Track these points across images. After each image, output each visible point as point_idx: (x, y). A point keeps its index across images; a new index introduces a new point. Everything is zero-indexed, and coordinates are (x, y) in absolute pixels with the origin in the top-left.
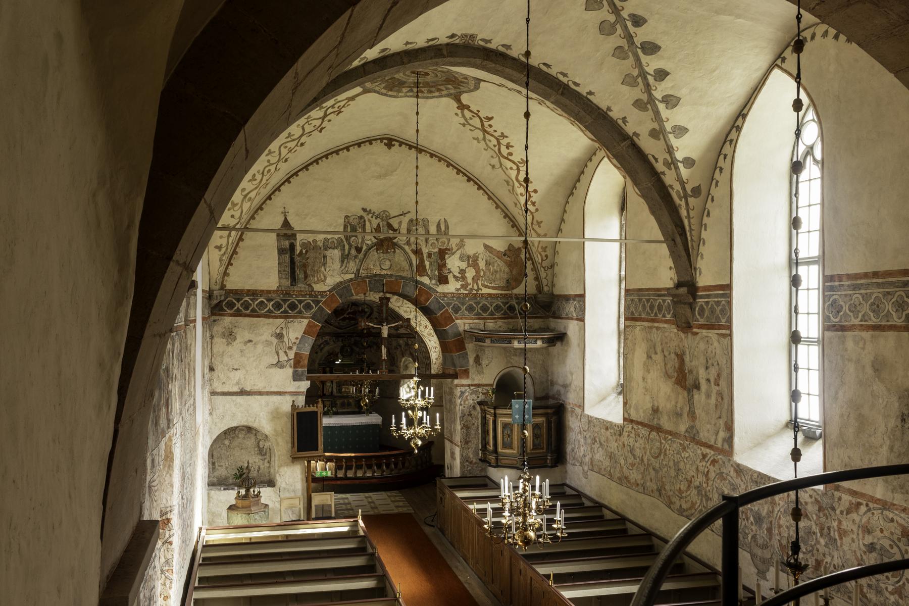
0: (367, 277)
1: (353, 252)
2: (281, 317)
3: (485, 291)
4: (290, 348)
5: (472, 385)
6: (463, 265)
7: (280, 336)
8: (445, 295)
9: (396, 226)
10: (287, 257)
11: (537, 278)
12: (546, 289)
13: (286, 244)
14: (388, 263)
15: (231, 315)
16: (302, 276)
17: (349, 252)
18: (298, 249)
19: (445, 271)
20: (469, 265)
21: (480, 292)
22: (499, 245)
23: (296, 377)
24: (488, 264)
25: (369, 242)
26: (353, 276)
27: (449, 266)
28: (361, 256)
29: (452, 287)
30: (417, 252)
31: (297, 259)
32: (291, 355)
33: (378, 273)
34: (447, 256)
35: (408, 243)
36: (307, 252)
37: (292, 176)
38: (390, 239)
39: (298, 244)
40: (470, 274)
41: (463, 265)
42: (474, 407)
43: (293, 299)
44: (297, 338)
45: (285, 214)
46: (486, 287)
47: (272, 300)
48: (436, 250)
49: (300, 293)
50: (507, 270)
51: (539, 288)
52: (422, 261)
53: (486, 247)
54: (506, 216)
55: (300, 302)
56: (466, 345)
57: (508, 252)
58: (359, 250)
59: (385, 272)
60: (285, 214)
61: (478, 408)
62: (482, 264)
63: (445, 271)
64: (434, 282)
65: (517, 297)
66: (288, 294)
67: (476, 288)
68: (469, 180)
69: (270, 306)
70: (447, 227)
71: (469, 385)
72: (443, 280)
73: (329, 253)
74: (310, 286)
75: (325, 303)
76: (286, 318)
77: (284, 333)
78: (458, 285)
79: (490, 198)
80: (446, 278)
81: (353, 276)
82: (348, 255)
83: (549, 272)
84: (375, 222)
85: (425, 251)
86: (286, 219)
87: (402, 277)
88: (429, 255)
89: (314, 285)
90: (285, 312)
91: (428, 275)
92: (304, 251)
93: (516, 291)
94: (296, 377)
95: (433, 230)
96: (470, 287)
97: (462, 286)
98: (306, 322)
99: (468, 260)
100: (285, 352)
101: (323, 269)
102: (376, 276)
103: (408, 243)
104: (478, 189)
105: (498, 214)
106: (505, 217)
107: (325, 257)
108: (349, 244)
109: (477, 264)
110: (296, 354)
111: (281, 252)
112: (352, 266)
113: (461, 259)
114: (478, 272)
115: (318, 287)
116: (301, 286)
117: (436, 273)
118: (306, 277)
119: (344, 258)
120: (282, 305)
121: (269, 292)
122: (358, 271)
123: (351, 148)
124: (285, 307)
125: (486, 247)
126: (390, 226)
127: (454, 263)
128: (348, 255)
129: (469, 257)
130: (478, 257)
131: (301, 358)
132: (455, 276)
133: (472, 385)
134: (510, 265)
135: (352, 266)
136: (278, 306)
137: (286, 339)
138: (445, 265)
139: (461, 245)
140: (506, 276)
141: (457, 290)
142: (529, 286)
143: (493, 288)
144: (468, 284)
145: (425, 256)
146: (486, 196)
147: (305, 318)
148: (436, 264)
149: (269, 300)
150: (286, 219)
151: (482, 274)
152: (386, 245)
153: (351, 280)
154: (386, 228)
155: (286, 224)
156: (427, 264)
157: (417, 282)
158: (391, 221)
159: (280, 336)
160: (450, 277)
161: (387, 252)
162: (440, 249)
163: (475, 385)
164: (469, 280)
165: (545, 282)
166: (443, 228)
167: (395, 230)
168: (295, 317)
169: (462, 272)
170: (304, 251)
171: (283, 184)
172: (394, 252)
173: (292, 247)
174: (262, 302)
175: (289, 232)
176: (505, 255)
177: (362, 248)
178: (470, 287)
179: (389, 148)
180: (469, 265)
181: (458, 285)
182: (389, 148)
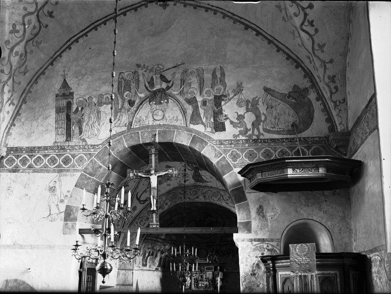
0: (139, 129)
1: (127, 105)
2: (54, 171)
3: (268, 136)
4: (62, 201)
5: (255, 240)
6: (242, 111)
7: (52, 189)
8: (221, 142)
9: (169, 77)
10: (63, 116)
11: (330, 120)
12: (340, 128)
13: (64, 103)
14: (160, 113)
15: (10, 171)
16: (77, 131)
17: (122, 107)
18: (74, 107)
19: (221, 118)
20: (248, 110)
21: (261, 137)
22: (283, 88)
23: (66, 230)
24: (270, 107)
25: (142, 95)
26: (125, 128)
27: (225, 113)
28: (134, 109)
29: (230, 132)
30: (192, 101)
31: (73, 116)
32: (63, 208)
33: (151, 124)
34: (223, 103)
35: (181, 93)
36: (82, 109)
37: (72, 43)
38: (162, 91)
39: (75, 102)
40: (249, 118)
41: (242, 111)
42: (258, 265)
43: (68, 154)
44: (68, 192)
45: (64, 76)
46: (268, 131)
47: (49, 155)
48: (212, 97)
49: (73, 148)
50: (292, 112)
51: (332, 128)
52: (196, 109)
53: (267, 90)
54: (289, 57)
55: (74, 156)
56: (247, 195)
57: (291, 94)
58: (131, 103)
59: (158, 123)
60: (64, 76)
61: (262, 266)
62: (262, 109)
63: (221, 118)
64: (209, 129)
65: (305, 140)
66: (63, 148)
67: (256, 132)
68: (247, 27)
69: (46, 161)
70: (223, 74)
71: (251, 240)
72: (219, 127)
73: (102, 109)
74: (84, 140)
75: (97, 156)
76: (60, 171)
77: (57, 185)
78: (236, 131)
79: (270, 42)
80: (223, 124)
81: (125, 128)
82: (121, 109)
83: (342, 107)
84: (148, 75)
85: (199, 99)
86: (65, 80)
87: (175, 127)
88: (204, 103)
89: (87, 140)
90: (60, 166)
91: (203, 123)
92: (80, 109)
93: (306, 134)
94: (66, 230)
95: (208, 76)
96: (250, 133)
97: (241, 133)
98: (78, 174)
99: (247, 105)
100: (57, 205)
101: (97, 124)
102: (148, 127)
103: (181, 93)
104: (257, 35)
105: (281, 57)
106: (287, 59)
107: (99, 112)
108: (123, 98)
109: (257, 108)
110: (67, 207)
111: (58, 111)
112: (125, 119)
113: (239, 104)
114: (258, 117)
115: (90, 142)
116: (75, 141)
117: (212, 120)
118: (81, 132)
119: (117, 112)
120: (57, 159)
121: (46, 148)
122: (131, 124)
123: (128, 13)
124: (60, 161)
125: (267, 90)
126: (163, 78)
127: (230, 109)
128: (121, 109)
129: (248, 102)
130: (258, 101)
131: (72, 210)
132: (232, 122)
133: (255, 240)
134: (294, 107)
135: (125, 119)
136: (53, 161)
137: (58, 192)
138: (221, 112)
139: (239, 89)
140: (291, 120)
141: (235, 136)
142: (318, 128)
143: (278, 133)
144: (247, 130)
145: (199, 104)
146: (266, 42)
147: (77, 171)
148: (211, 112)
149: (45, 156)
150: (65, 80)
151: (263, 118)
152: (157, 96)
153: (122, 133)
154: (159, 80)
155: (65, 85)
156: (201, 111)
157: (191, 131)
158: (165, 74)
159: (52, 189)
160: (227, 124)
161: (161, 103)
162: (216, 97)
163: (259, 240)
164: (249, 126)
165: (337, 120)
166: (218, 75)
167: (167, 81)
168: (68, 171)
169: (240, 117)
170: (80, 109)
171: (64, 50)
172: (168, 102)
173: (69, 105)
174: (39, 157)
175: (67, 93)
176: (289, 97)
177: (134, 102)
178: (250, 133)
179: (165, 8)
180: (248, 110)
181: (236, 131)
182: (165, 8)
